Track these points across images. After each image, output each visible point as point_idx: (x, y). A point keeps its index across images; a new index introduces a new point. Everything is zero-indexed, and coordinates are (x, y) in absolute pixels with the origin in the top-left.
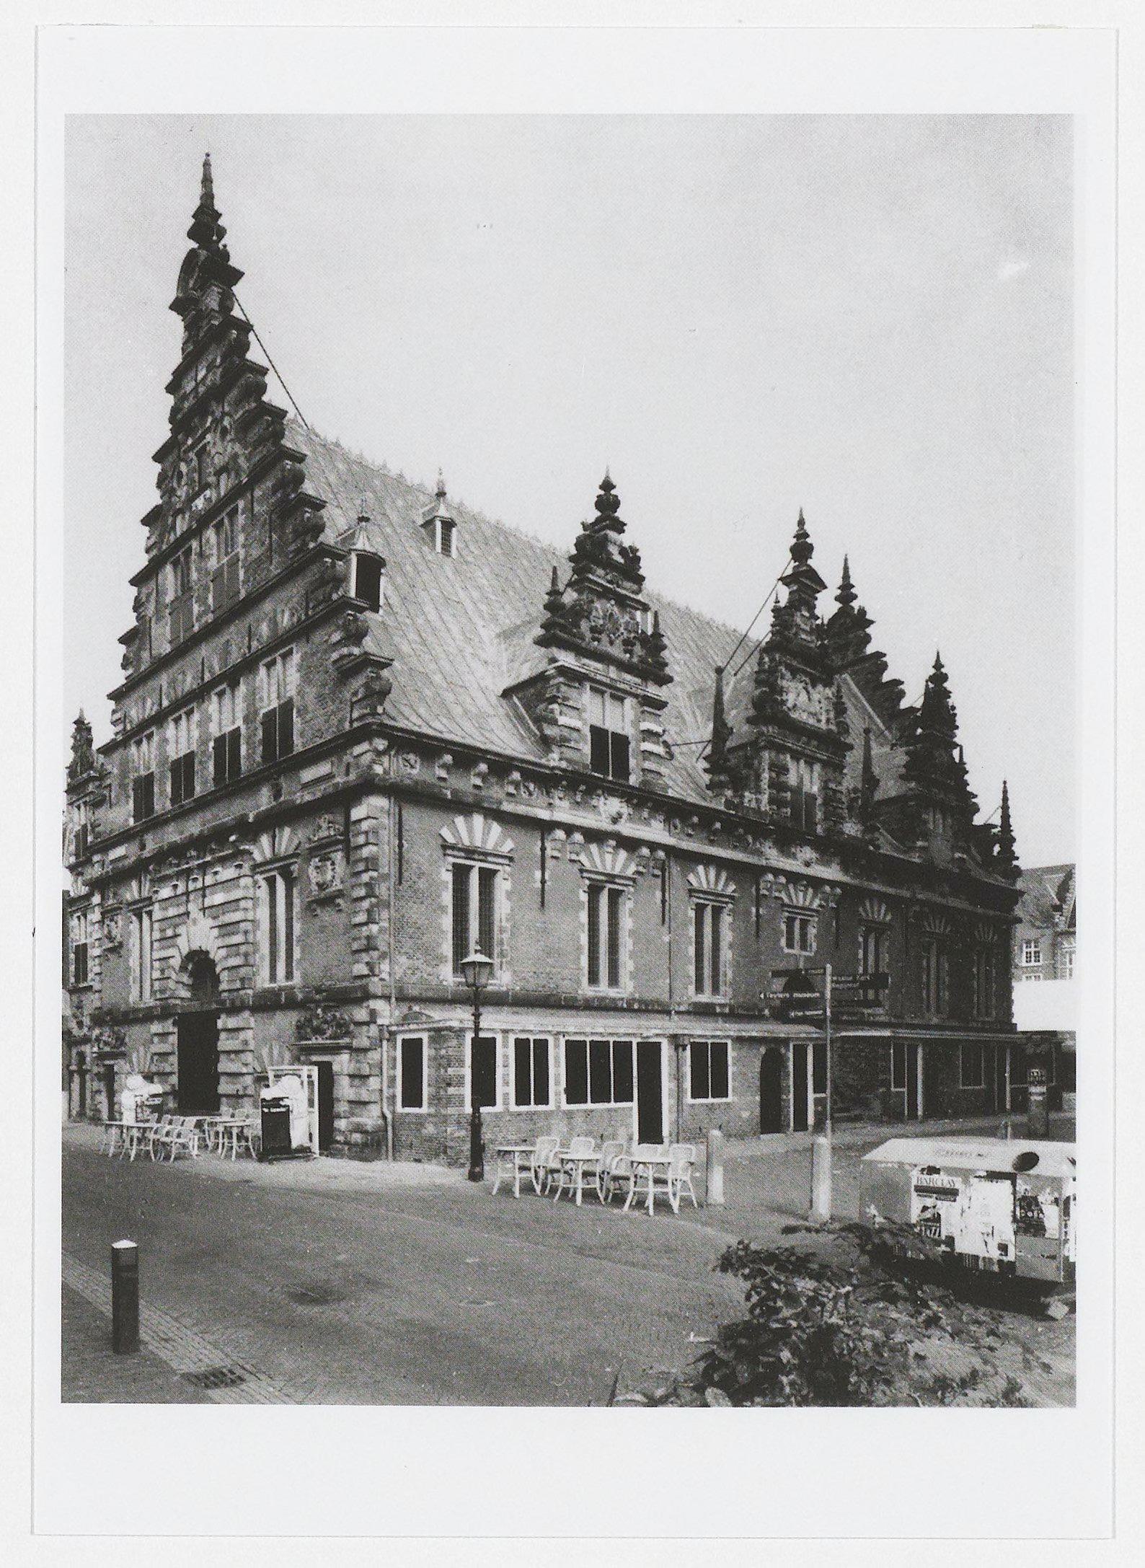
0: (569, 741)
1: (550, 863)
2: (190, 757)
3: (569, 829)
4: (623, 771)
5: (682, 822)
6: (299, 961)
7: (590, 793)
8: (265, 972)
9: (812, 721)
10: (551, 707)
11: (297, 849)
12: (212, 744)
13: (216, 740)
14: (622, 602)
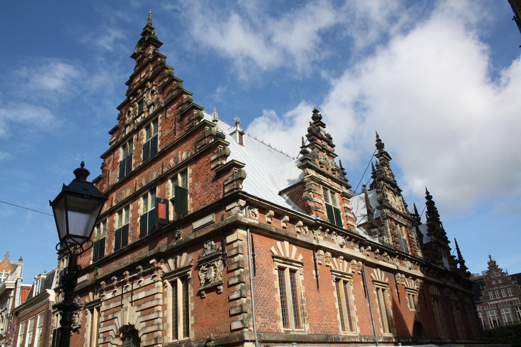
0: (319, 209)
3: (325, 250)
5: (365, 248)
6: (193, 325)
7: (330, 233)
8: (170, 334)
10: (309, 193)
11: (191, 263)
12: (139, 219)
14: (329, 153)
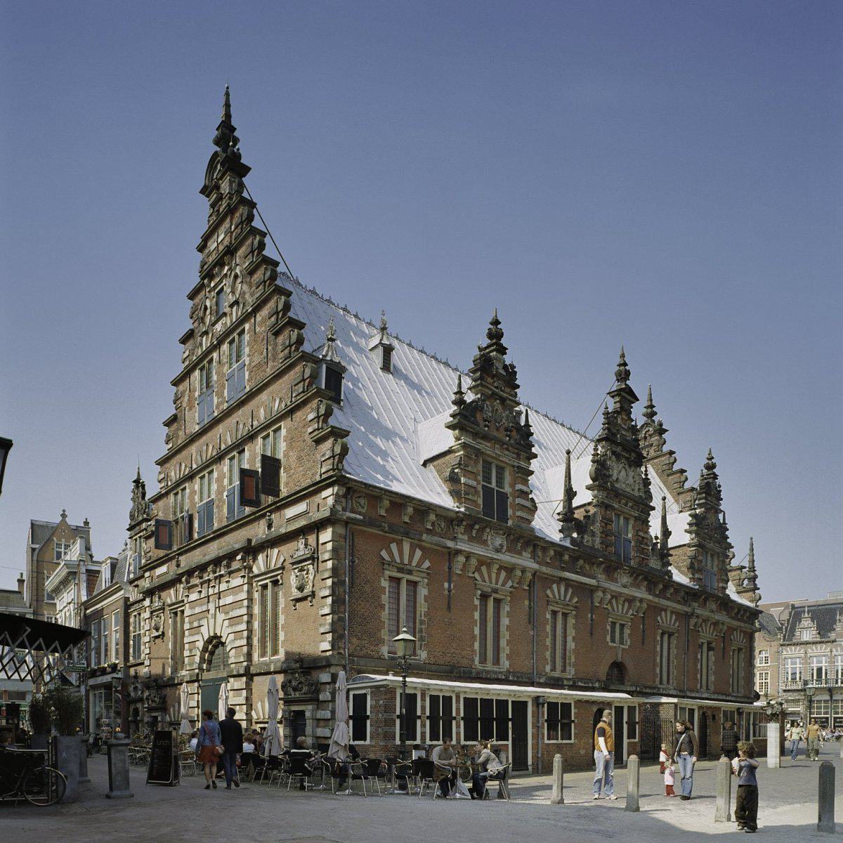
1: (455, 578)
2: (210, 504)
4: (503, 517)
9: (628, 490)
12: (225, 494)
13: (229, 491)
